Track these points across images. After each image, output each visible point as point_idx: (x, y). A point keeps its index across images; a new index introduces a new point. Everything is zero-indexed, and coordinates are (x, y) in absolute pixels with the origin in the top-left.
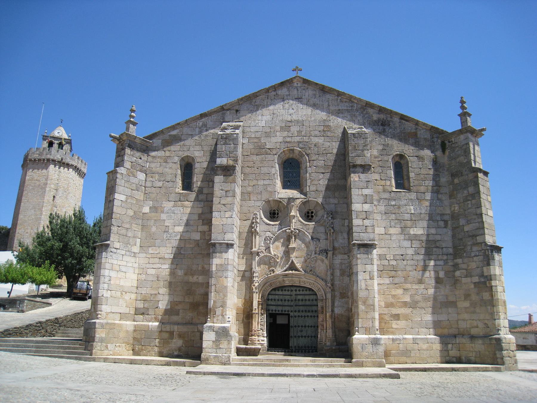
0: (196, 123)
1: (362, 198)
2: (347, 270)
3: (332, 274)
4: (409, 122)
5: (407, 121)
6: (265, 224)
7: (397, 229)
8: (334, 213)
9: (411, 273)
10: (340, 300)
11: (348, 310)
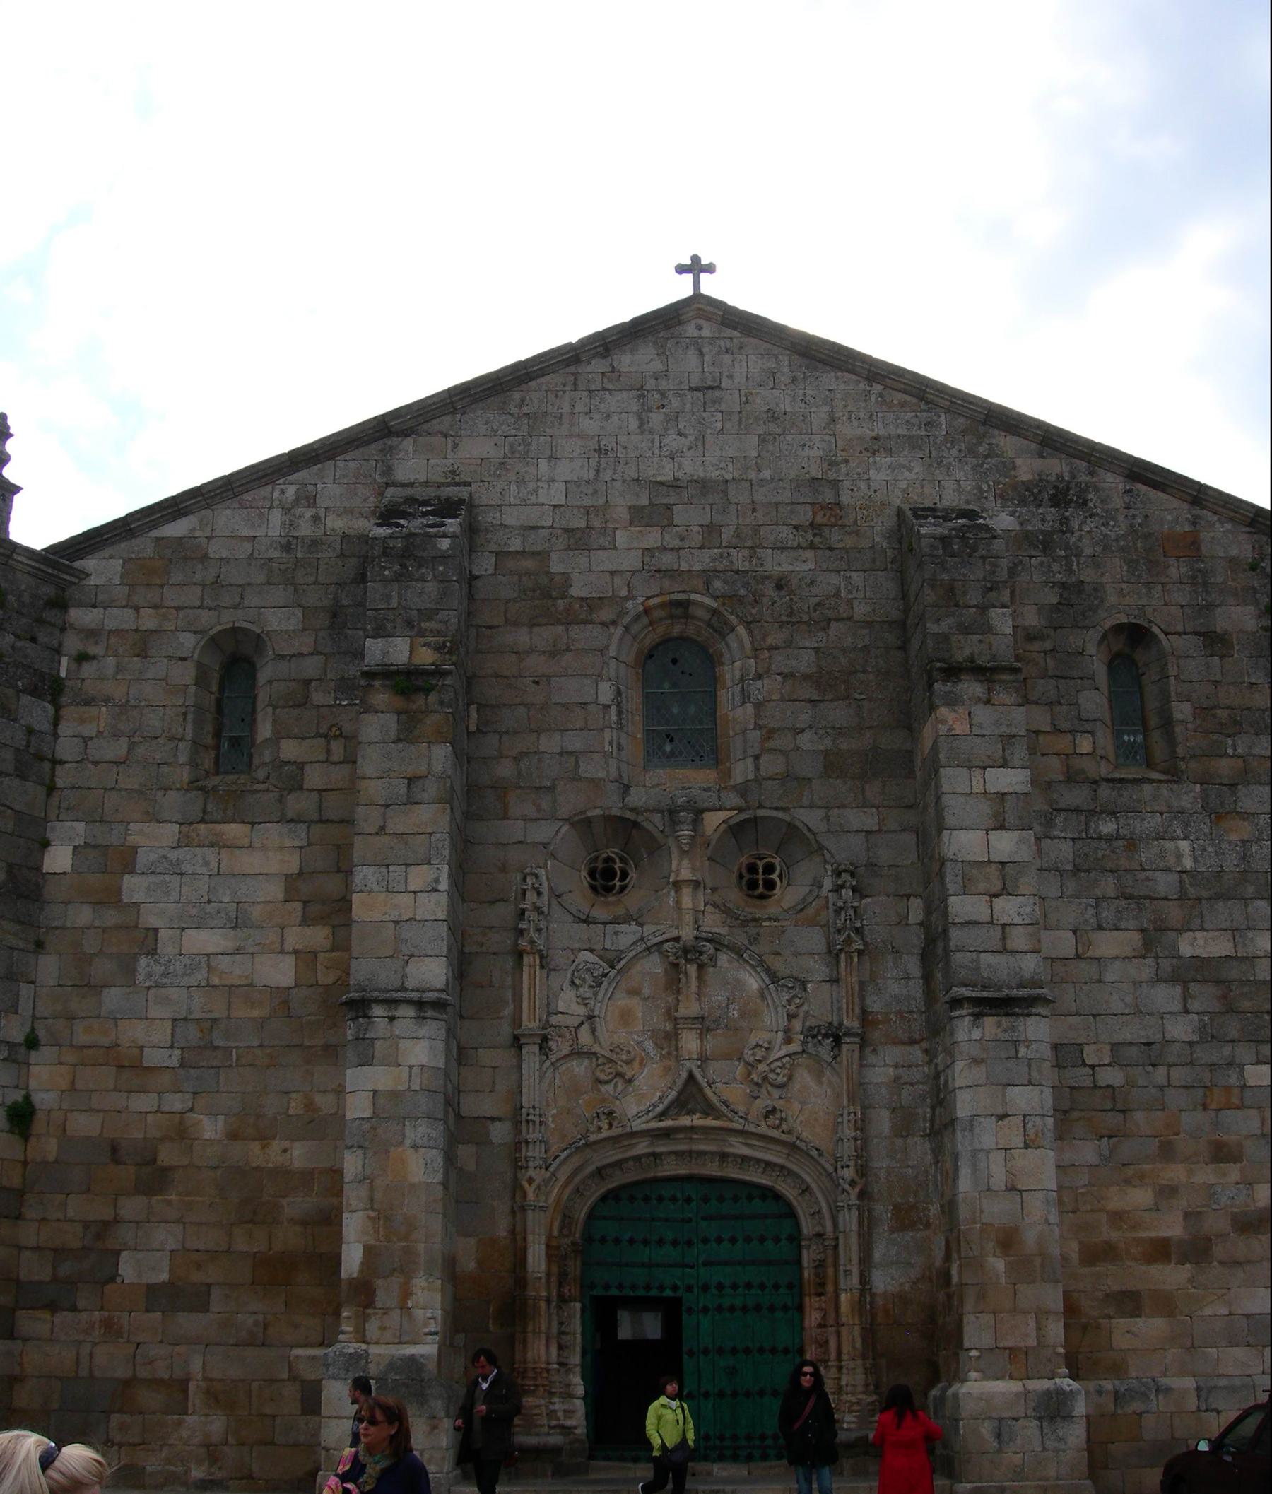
0: (270, 487)
1: (985, 808)
2: (920, 1111)
3: (862, 1125)
4: (1164, 491)
5: (1156, 486)
6: (571, 918)
7: (1128, 934)
8: (862, 870)
9: (1185, 1117)
10: (895, 1235)
11: (930, 1279)
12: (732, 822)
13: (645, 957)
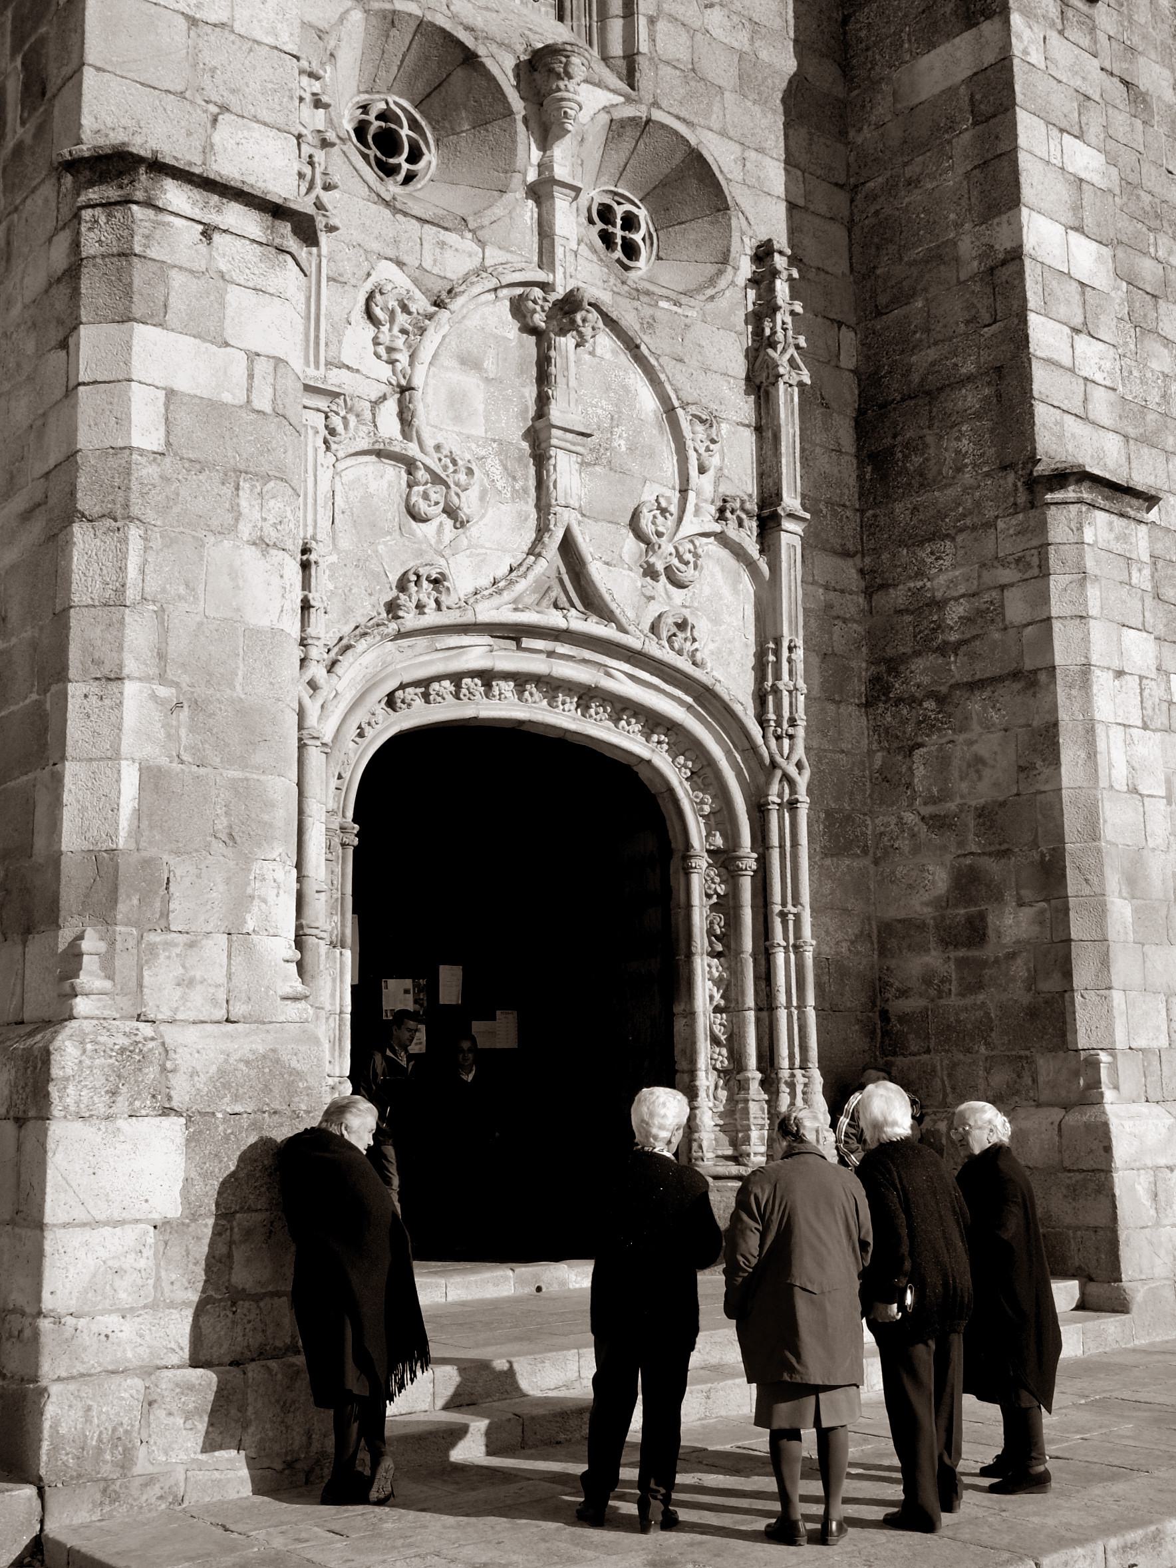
2: (854, 664)
10: (828, 862)
12: (618, 114)
13: (487, 303)
